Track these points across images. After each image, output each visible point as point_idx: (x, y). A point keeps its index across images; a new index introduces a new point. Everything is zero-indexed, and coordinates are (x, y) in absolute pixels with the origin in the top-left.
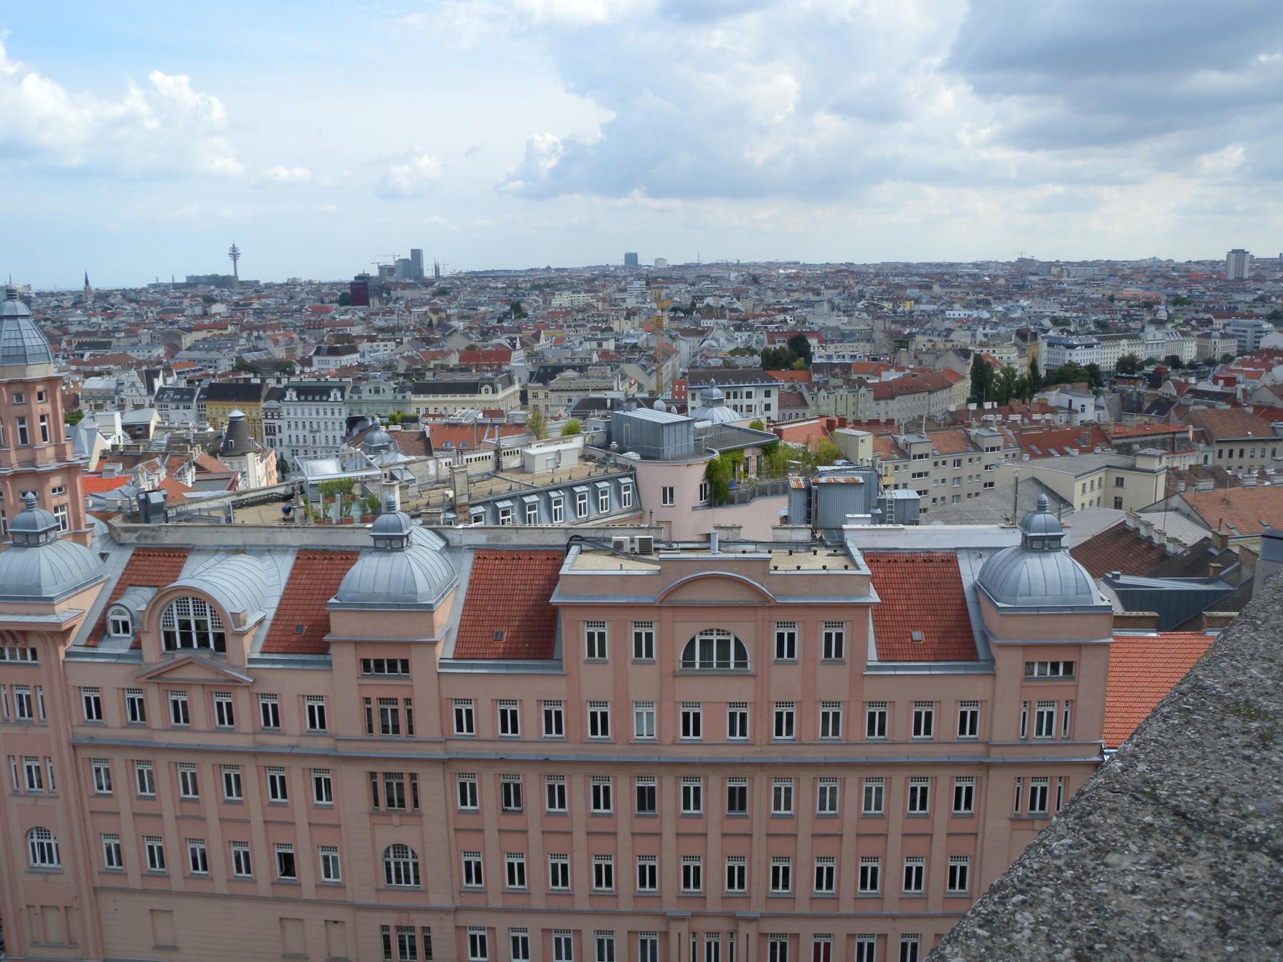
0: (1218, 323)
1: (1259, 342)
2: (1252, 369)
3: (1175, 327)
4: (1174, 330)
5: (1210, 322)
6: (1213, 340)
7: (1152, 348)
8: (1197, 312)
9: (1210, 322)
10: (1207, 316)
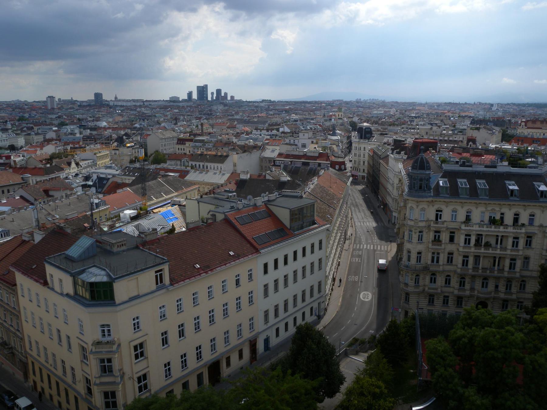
0: (36, 128)
1: (45, 136)
2: (33, 149)
3: (13, 131)
4: (12, 133)
5: (32, 128)
6: (32, 136)
7: (4, 141)
8: (27, 124)
9: (32, 128)
10: (31, 125)
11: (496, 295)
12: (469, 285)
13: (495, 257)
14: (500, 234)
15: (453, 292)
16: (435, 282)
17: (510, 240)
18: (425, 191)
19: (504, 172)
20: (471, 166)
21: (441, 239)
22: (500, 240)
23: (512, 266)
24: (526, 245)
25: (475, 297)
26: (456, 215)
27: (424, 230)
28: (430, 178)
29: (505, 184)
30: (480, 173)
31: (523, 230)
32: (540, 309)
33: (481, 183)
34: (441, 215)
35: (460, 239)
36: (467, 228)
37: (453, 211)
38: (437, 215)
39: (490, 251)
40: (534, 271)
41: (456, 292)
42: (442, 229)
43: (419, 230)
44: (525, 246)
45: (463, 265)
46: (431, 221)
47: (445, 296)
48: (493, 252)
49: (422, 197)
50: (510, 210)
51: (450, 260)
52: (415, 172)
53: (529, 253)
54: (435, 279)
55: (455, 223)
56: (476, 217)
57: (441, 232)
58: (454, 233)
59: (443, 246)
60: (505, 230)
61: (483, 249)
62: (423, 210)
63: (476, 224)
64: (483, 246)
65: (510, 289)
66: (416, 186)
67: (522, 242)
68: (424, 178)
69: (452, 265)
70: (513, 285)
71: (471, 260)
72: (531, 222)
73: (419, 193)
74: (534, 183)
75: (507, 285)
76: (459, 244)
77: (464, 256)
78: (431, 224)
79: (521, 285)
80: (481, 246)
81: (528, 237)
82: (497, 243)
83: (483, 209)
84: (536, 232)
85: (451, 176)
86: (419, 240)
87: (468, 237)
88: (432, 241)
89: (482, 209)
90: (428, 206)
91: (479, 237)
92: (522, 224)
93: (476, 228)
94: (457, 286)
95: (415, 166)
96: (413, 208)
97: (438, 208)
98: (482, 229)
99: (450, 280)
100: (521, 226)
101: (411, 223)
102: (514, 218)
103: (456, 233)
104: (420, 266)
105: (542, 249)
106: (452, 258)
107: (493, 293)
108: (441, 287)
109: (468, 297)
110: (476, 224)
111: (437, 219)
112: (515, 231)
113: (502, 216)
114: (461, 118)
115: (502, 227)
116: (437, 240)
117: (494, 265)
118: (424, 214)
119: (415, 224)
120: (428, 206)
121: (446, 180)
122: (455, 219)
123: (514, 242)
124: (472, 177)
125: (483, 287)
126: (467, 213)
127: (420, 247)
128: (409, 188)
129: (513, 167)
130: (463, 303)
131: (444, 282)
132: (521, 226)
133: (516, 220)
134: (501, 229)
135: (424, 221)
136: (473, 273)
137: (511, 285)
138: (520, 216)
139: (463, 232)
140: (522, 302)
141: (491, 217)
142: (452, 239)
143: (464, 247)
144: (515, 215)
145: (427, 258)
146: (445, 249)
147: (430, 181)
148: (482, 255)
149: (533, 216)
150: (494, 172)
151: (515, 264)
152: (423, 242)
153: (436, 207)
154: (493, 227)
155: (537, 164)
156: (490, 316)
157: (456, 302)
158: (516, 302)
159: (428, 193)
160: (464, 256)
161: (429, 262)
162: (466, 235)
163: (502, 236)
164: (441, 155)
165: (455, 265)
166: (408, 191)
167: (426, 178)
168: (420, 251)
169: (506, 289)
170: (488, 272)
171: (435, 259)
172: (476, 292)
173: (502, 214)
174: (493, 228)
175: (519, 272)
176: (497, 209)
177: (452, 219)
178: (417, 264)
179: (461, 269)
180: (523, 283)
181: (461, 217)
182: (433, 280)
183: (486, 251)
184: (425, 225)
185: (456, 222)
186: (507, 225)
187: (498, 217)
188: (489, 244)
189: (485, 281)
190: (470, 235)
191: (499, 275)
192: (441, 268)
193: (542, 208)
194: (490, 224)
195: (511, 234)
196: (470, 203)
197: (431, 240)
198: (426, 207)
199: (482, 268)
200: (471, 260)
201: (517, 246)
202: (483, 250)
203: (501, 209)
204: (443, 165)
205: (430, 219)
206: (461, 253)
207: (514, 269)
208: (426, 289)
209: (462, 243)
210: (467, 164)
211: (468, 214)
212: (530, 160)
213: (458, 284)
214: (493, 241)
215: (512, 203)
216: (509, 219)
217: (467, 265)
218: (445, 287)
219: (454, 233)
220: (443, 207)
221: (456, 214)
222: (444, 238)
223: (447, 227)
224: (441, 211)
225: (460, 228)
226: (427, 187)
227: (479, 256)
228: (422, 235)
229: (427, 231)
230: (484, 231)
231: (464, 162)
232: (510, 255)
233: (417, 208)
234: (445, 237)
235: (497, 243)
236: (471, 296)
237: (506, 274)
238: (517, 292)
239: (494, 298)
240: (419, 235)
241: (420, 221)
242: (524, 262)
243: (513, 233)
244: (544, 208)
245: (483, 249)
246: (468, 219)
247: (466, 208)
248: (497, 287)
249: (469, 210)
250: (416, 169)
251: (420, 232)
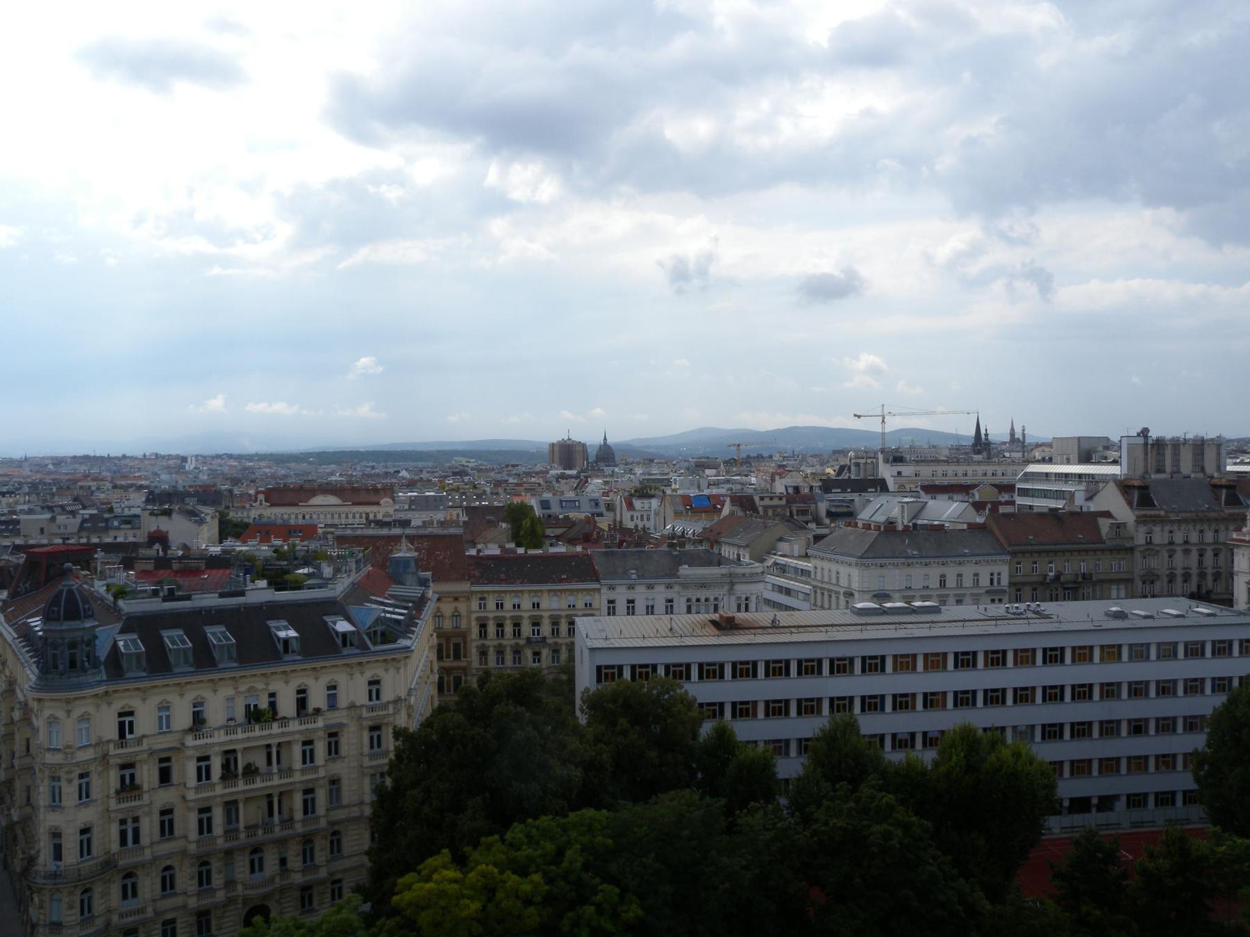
11: (285, 882)
12: (221, 876)
13: (270, 796)
14: (274, 742)
15: (185, 906)
16: (135, 894)
17: (297, 750)
18: (84, 670)
19: (262, 603)
20: (188, 598)
21: (138, 781)
22: (276, 753)
23: (309, 807)
24: (330, 753)
25: (240, 901)
26: (168, 717)
27: (92, 768)
28: (95, 637)
29: (268, 628)
30: (211, 611)
31: (320, 723)
32: (400, 881)
33: (216, 634)
34: (131, 723)
35: (187, 770)
36: (199, 742)
37: (160, 709)
38: (122, 725)
39: (259, 784)
40: (354, 805)
41: (193, 903)
42: (138, 758)
43: (78, 771)
44: (327, 757)
45: (201, 832)
46: (109, 741)
47: (165, 923)
48: (265, 784)
49: (80, 687)
50: (287, 682)
51: (167, 827)
52: (52, 628)
54: (134, 886)
55: (168, 735)
56: (215, 713)
57: (138, 766)
58: (168, 759)
59: (146, 797)
60: (284, 730)
61: (241, 783)
62: (85, 718)
63: (219, 729)
64: (240, 777)
65: (312, 859)
66: (59, 662)
67: (320, 749)
68: (79, 639)
69: (175, 839)
70: (317, 848)
71: (218, 815)
73: (69, 677)
74: (325, 618)
75: (304, 851)
76: (185, 785)
77: (201, 811)
78: (108, 750)
79: (332, 843)
80: (236, 776)
81: (331, 735)
82: (269, 762)
83: (229, 691)
84: (345, 721)
85: (146, 626)
86: (80, 798)
87: (203, 764)
88: (117, 792)
89: (226, 691)
90: (98, 706)
91: (229, 757)
92: (314, 709)
93: (220, 737)
94: (192, 886)
95: (53, 611)
96: (57, 718)
97: (123, 708)
98: (233, 737)
99: (172, 877)
100: (313, 715)
101: (57, 758)
102: (298, 699)
103: (173, 759)
104: (95, 861)
105: (362, 754)
106: (171, 822)
107: (277, 879)
108: (154, 901)
109: (224, 906)
110: (219, 729)
111: (122, 735)
112: (303, 727)
113: (272, 699)
114: (119, 490)
115: (275, 725)
116: (129, 787)
117: (271, 814)
118: (88, 728)
119: (66, 759)
120: (98, 706)
121: (135, 636)
122: (168, 727)
123: (304, 752)
124: (194, 622)
125: (252, 871)
126: (194, 707)
127: (88, 815)
128: (41, 671)
129: (277, 590)
130: (214, 923)
131: (158, 886)
132: (313, 715)
133: (302, 703)
134: (276, 728)
135: (90, 745)
136: (228, 845)
137: (312, 850)
138: (308, 692)
139: (190, 752)
140: (340, 881)
141: (250, 705)
142: (165, 776)
143: (197, 789)
144: (329, 688)
145: (107, 839)
146: (151, 803)
147: (95, 645)
148: (241, 797)
149: (334, 688)
150: (240, 605)
151: (313, 800)
152: (92, 801)
153: (118, 705)
154: (257, 727)
155: (322, 578)
156: (302, 931)
157: (195, 929)
158: (329, 885)
159: (93, 674)
160: (201, 811)
161: (115, 847)
162: (200, 759)
163: (279, 745)
164: (109, 581)
165: (181, 838)
166: (39, 678)
167: (85, 639)
168: (88, 826)
169: (305, 861)
170: (260, 832)
171: (129, 834)
172: (240, 887)
173: (272, 695)
174: (257, 732)
175: (324, 816)
176: (260, 686)
177: (161, 728)
178: (82, 862)
179: (197, 842)
180: (335, 838)
181: (182, 719)
182: (130, 891)
183: (248, 787)
184: (93, 756)
185: (171, 732)
186: (285, 718)
187: (264, 704)
188: (253, 768)
189: (256, 857)
190: (207, 758)
191: (286, 833)
192: (148, 854)
193: (348, 669)
194: (250, 723)
195: (297, 737)
196: (252, 676)
197: (112, 791)
198: (91, 710)
199: (247, 828)
200: (218, 815)
201: (312, 761)
202: (241, 786)
203: (267, 684)
204: (121, 603)
205: (104, 739)
206: (192, 804)
207: (313, 811)
208: (115, 918)
209: (192, 781)
210: (180, 593)
211: (196, 709)
212: (306, 571)
213: (196, 881)
214: (260, 761)
215: (288, 668)
216: (287, 706)
217: (210, 830)
218: (163, 897)
219: (168, 759)
220: (135, 703)
221: (167, 713)
222: (145, 779)
223: (150, 749)
224: (131, 713)
225: (183, 744)
226: (88, 661)
227: (235, 802)
228: (88, 783)
229: (100, 769)
230: (237, 741)
231: (171, 591)
232: (302, 782)
233: (69, 716)
234: (147, 775)
235: (269, 762)
236: (230, 901)
237: (299, 828)
238: (327, 861)
239: (282, 890)
240: (80, 786)
241: (80, 748)
242: (331, 791)
243: (300, 732)
244: (352, 668)
245: (241, 783)
246: (198, 720)
247: (190, 696)
248: (283, 861)
249: (199, 700)
250: (58, 619)
251: (82, 776)
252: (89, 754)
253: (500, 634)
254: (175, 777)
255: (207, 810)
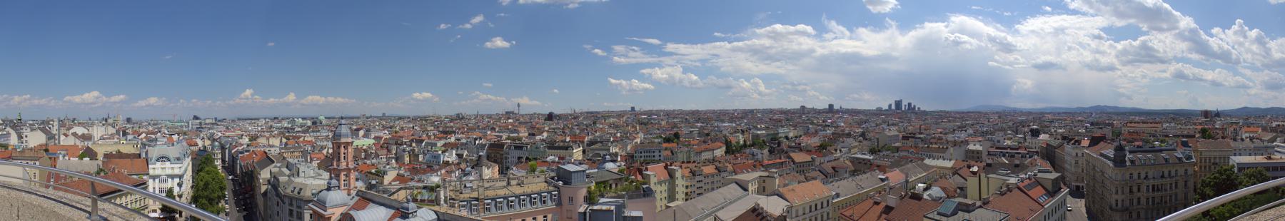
23: (1171, 200)
31: (1174, 179)
51: (1139, 202)
53: (1177, 190)
72: (1176, 174)
91: (1153, 186)
116: (1131, 191)
142: (1139, 190)
145: (1127, 203)
153: (1130, 172)
171: (1131, 201)
181: (1143, 176)
192: (1135, 208)
209: (1145, 191)
220: (1133, 172)
234: (1135, 189)
252: (1123, 183)
253: (1205, 162)
254: (1141, 190)
255: (1148, 199)
